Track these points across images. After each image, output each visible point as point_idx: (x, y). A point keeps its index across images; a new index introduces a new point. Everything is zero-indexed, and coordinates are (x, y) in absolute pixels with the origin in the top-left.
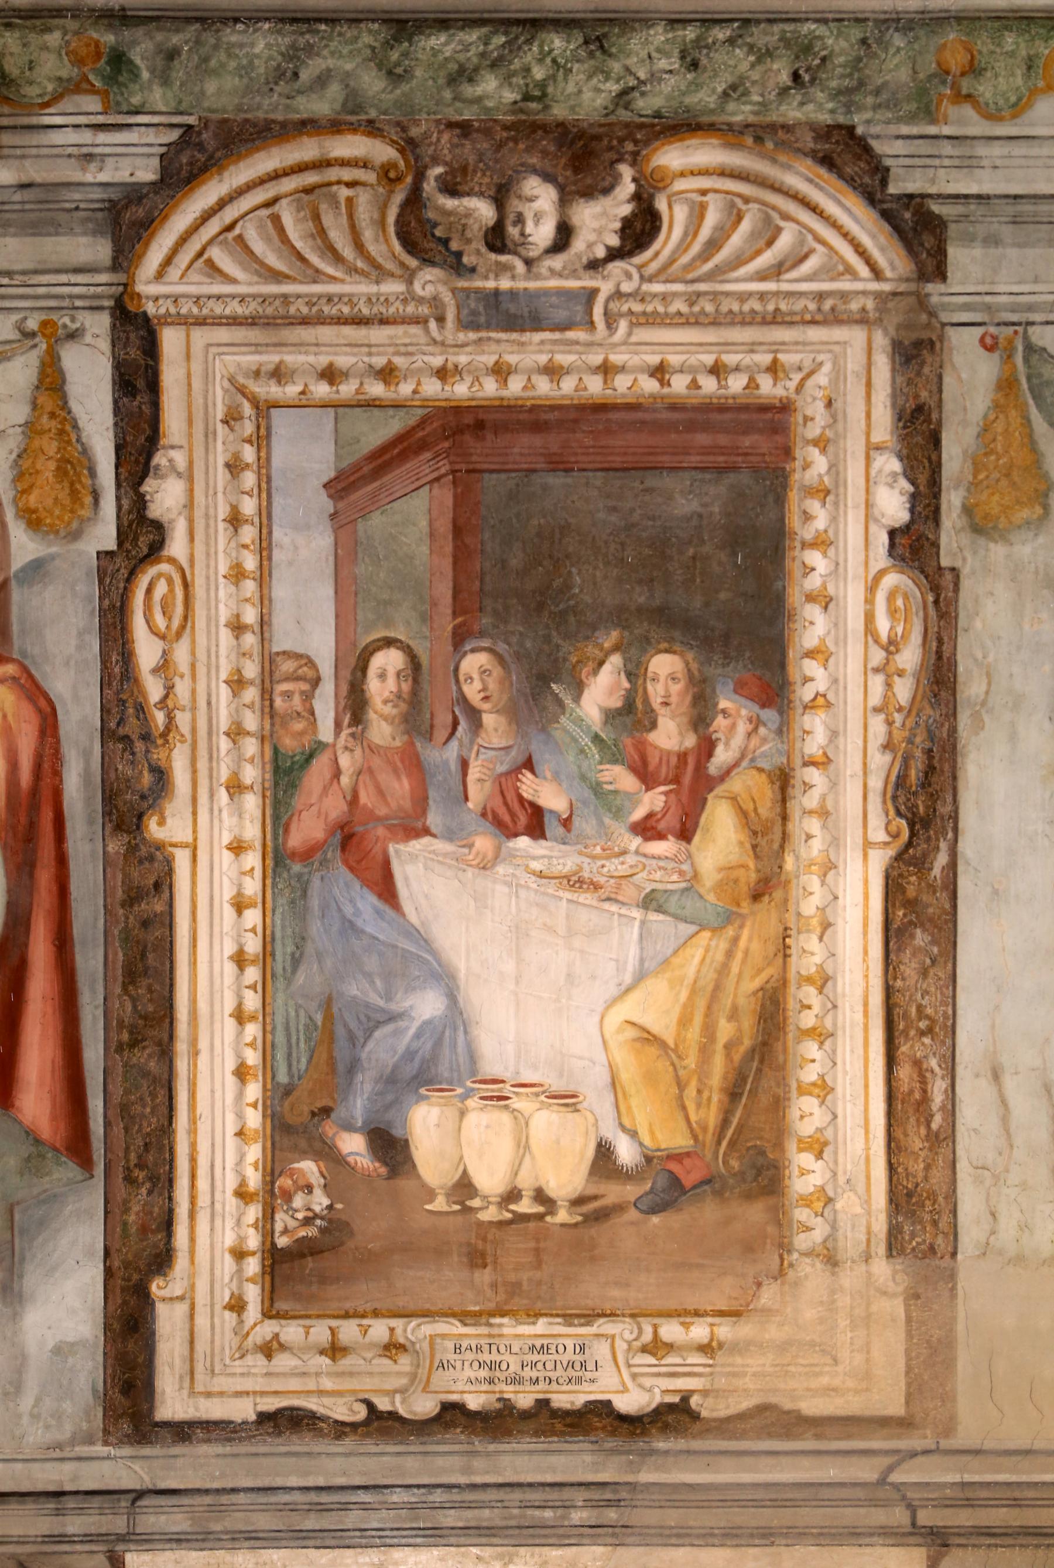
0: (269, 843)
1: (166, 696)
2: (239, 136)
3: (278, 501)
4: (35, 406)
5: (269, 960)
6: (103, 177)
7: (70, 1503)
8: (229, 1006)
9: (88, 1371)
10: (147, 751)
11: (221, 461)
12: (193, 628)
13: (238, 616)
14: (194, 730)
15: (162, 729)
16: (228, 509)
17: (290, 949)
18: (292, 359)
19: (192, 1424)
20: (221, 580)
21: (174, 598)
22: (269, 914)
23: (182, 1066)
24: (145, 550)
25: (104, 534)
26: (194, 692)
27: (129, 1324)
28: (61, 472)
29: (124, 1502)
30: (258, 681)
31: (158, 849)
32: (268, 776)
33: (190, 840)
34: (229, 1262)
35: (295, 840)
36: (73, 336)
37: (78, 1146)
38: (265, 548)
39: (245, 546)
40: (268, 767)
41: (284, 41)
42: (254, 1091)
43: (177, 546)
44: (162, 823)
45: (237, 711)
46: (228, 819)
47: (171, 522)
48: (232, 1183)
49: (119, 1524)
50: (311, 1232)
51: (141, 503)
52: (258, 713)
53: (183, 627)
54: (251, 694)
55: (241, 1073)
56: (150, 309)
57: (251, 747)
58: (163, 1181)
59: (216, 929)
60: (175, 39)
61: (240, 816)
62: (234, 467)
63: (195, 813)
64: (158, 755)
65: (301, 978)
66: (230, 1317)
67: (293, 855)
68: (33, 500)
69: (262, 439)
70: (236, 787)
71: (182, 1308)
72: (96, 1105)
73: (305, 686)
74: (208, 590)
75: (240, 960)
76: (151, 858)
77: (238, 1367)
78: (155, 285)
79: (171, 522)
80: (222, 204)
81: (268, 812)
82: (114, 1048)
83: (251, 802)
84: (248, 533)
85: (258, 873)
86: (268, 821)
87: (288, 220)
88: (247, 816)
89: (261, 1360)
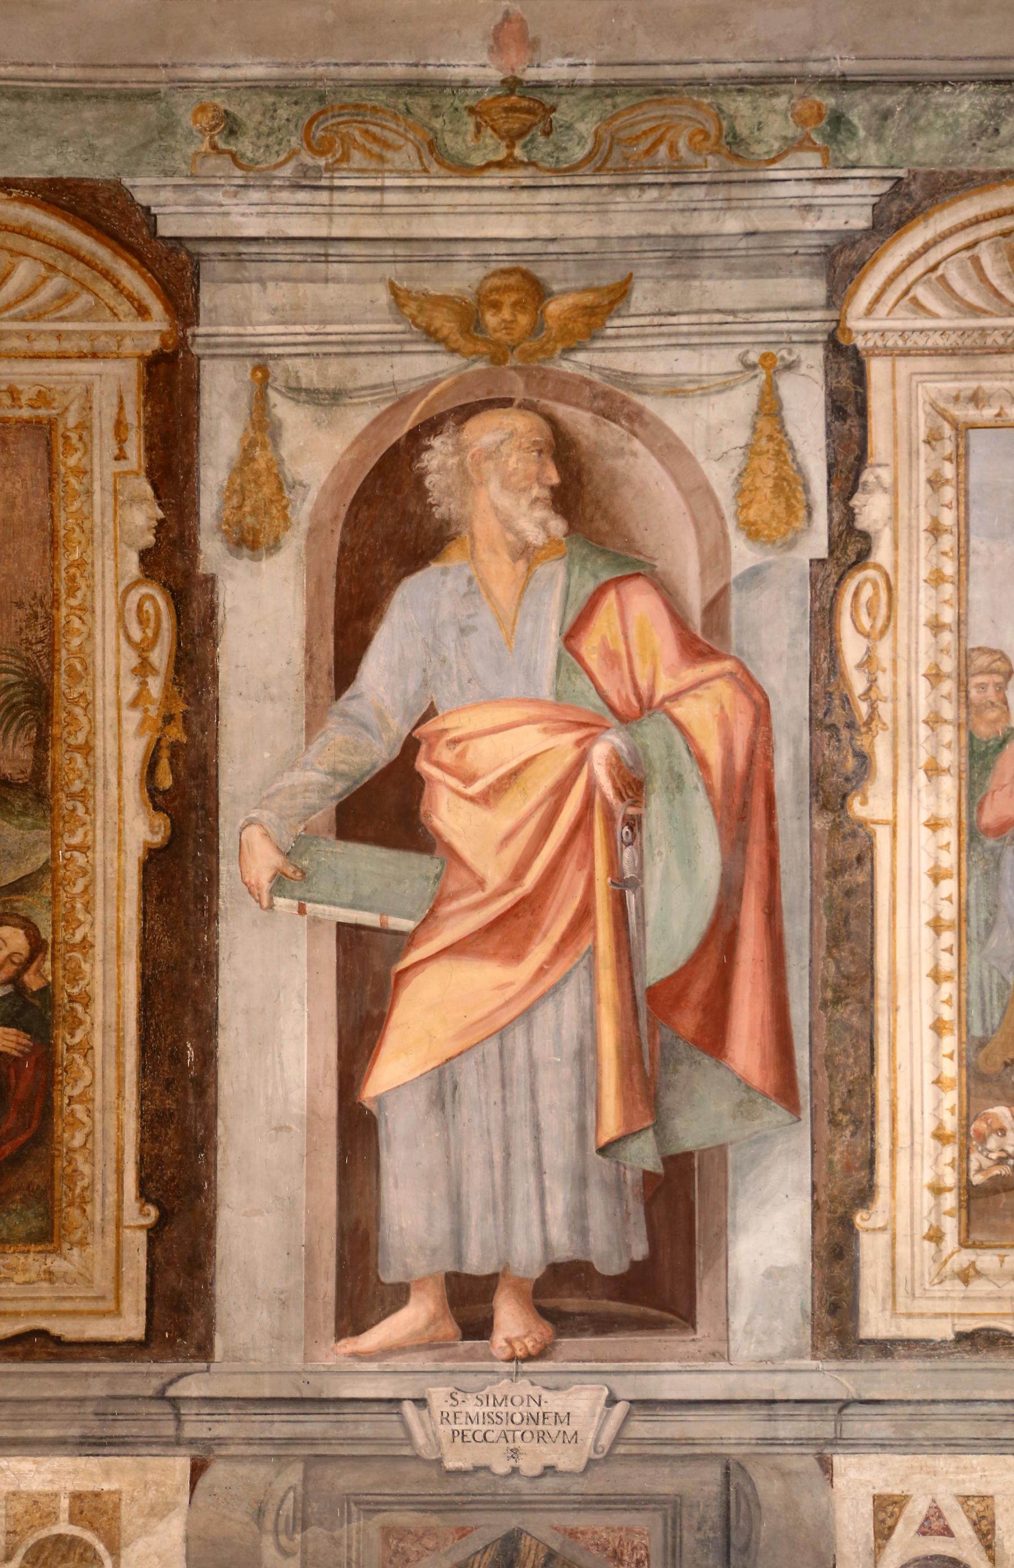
0: (964, 820)
1: (870, 689)
2: (944, 187)
3: (975, 513)
4: (754, 429)
5: (964, 925)
6: (820, 225)
7: (781, 1410)
8: (927, 966)
9: (798, 1293)
10: (852, 738)
11: (923, 477)
12: (895, 627)
13: (937, 616)
14: (895, 719)
15: (865, 718)
16: (929, 520)
17: (983, 915)
18: (988, 385)
19: (893, 1342)
20: (922, 584)
21: (879, 601)
22: (964, 884)
23: (882, 1021)
24: (853, 558)
25: (817, 543)
26: (895, 685)
27: (835, 1252)
28: (778, 489)
29: (832, 1411)
30: (955, 675)
31: (860, 826)
32: (963, 760)
33: (890, 818)
34: (928, 1197)
35: (989, 817)
36: (789, 367)
37: (786, 1092)
38: (963, 554)
39: (944, 554)
40: (964, 752)
41: (987, 101)
42: (950, 1043)
43: (882, 554)
44: (864, 802)
45: (935, 701)
46: (926, 800)
47: (877, 532)
48: (930, 1126)
49: (827, 1430)
50: (1004, 1170)
51: (850, 515)
52: (955, 703)
53: (886, 626)
54: (948, 686)
55: (938, 1027)
56: (860, 342)
57: (948, 733)
58: (865, 1124)
59: (914, 898)
60: (889, 101)
61: (938, 796)
62: (935, 483)
63: (895, 794)
64: (862, 742)
65: (994, 942)
66: (929, 1247)
67: (987, 831)
68: (752, 514)
69: (961, 457)
70: (934, 770)
71: (884, 1238)
72: (802, 1056)
73: (999, 679)
74: (910, 593)
75: (936, 926)
76: (854, 834)
77: (938, 1291)
78: (865, 320)
79: (877, 532)
80: (926, 248)
81: (964, 793)
82: (819, 1005)
83: (948, 784)
84: (948, 542)
85: (954, 847)
86: (964, 800)
87: (986, 261)
88: (944, 796)
89: (959, 1285)
